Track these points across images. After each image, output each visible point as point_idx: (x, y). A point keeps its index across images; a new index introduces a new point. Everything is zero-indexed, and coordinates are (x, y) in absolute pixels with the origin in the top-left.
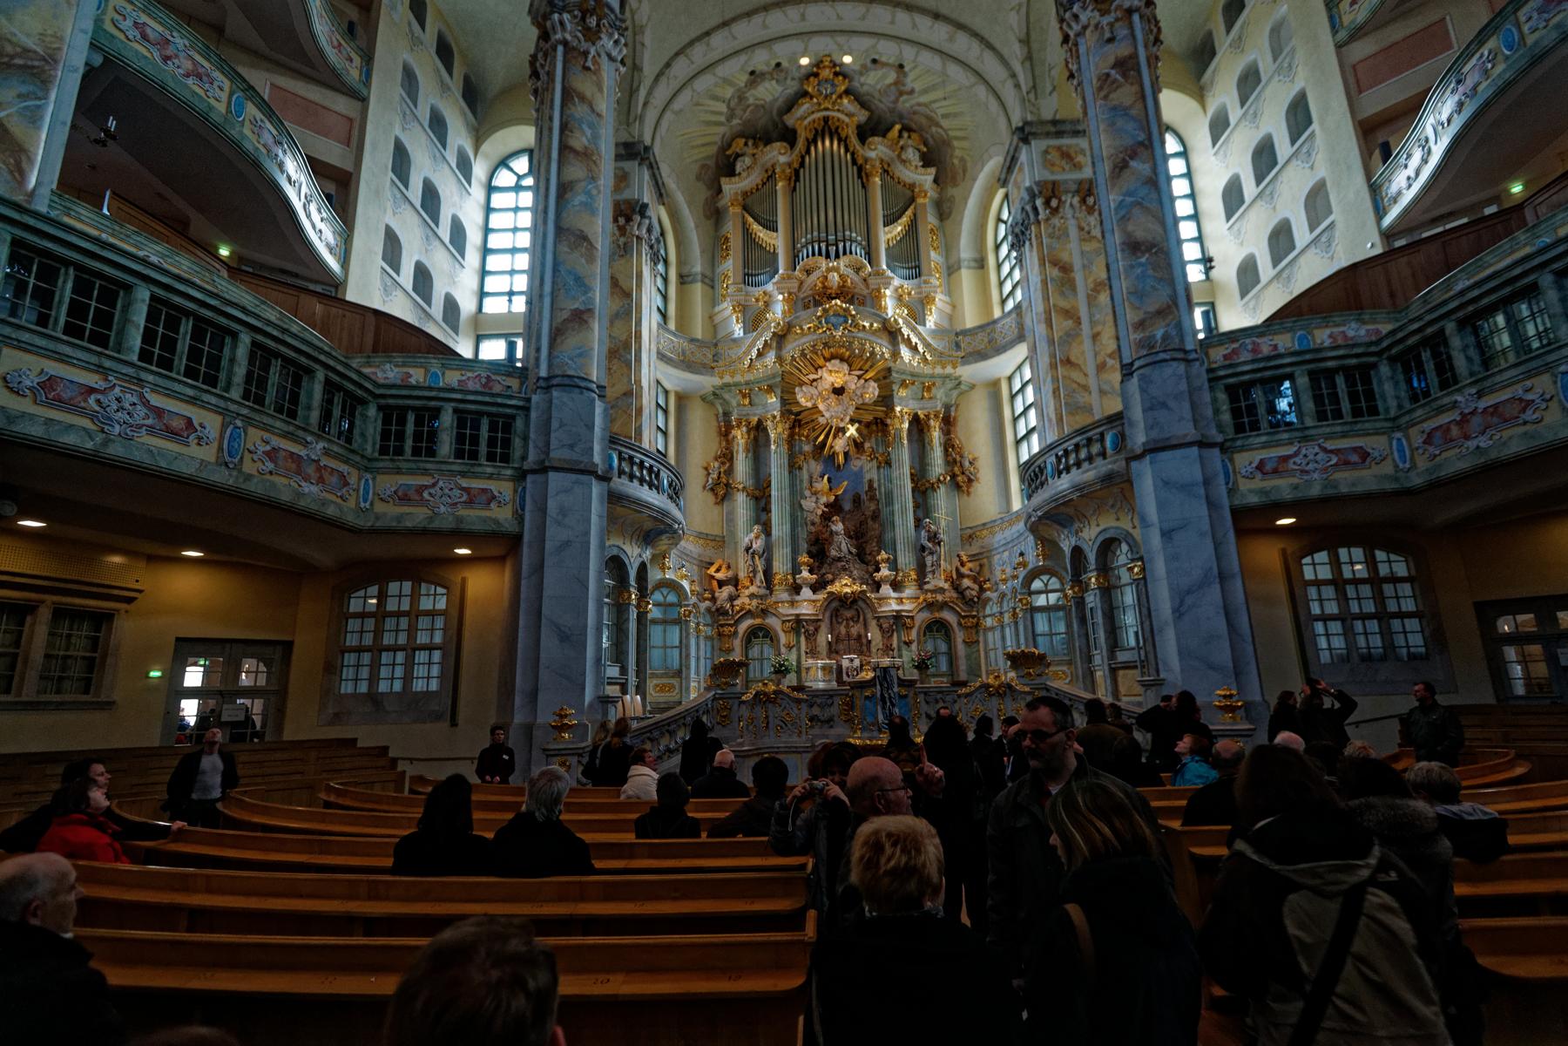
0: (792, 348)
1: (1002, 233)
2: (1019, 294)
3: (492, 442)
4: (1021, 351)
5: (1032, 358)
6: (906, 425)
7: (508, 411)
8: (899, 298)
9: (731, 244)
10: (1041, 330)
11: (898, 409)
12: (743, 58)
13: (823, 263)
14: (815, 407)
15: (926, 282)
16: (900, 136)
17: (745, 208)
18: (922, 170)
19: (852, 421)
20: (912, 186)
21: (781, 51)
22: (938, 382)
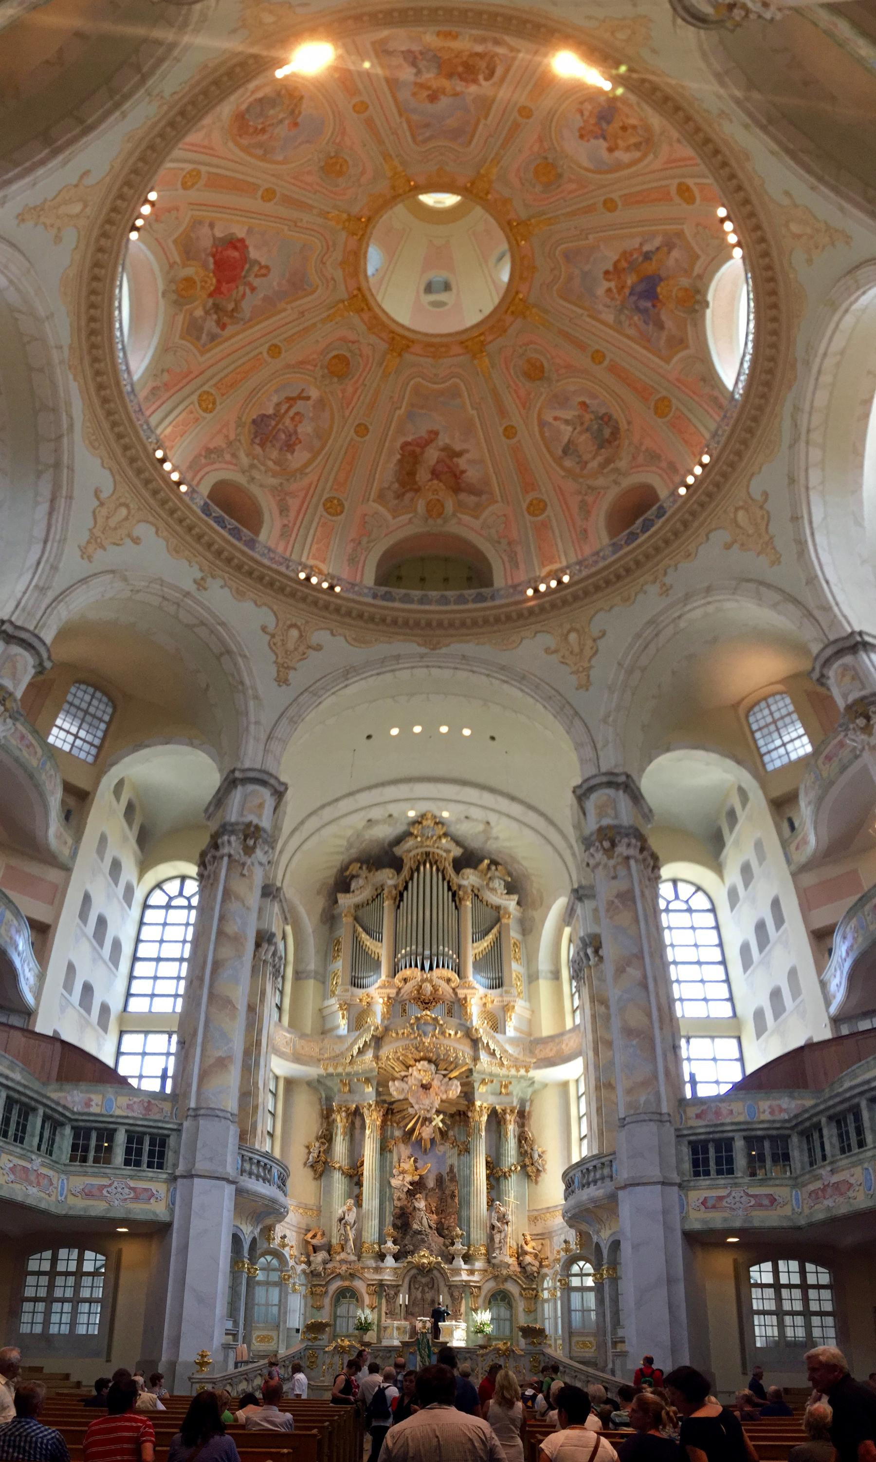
0: (387, 1051)
3: (151, 1154)
6: (485, 1118)
7: (166, 1132)
9: (343, 946)
10: (591, 1054)
11: (478, 1103)
12: (362, 814)
13: (417, 972)
14: (406, 1099)
15: (507, 992)
17: (356, 919)
18: (507, 897)
19: (438, 1112)
20: (498, 908)
21: (393, 809)
22: (514, 1082)
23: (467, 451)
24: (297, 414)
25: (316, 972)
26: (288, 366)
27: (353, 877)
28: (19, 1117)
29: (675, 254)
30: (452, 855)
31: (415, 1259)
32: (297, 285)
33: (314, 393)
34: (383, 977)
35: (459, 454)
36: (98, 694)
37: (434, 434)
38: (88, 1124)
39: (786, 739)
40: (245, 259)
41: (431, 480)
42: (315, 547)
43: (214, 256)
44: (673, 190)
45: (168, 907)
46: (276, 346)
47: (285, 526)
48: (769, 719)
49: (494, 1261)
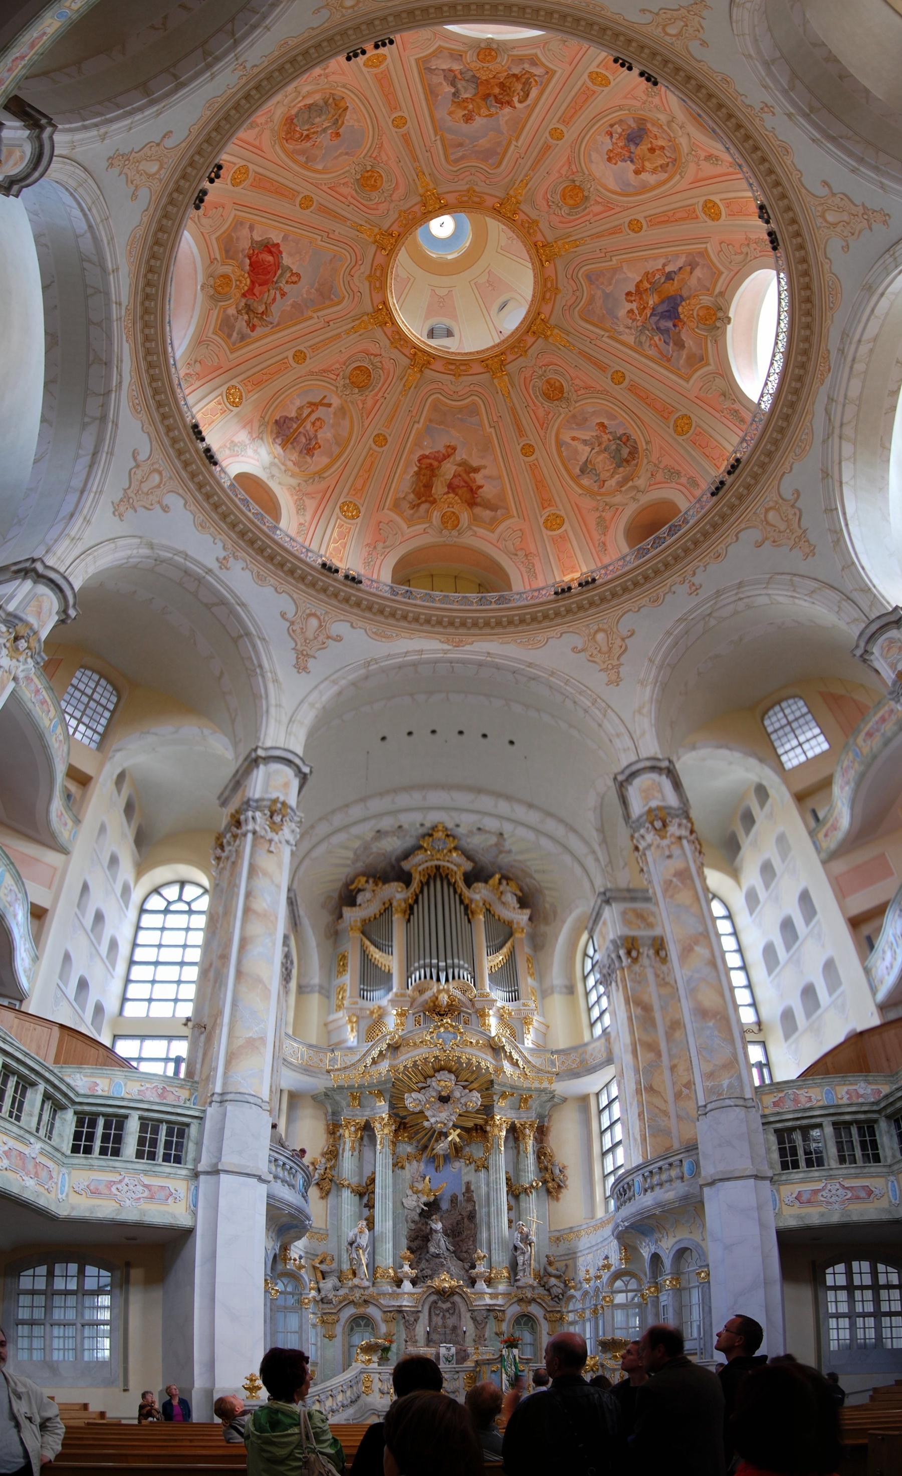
1: (588, 966)
2: (607, 1019)
4: (609, 1072)
5: (619, 1077)
8: (501, 1018)
10: (628, 1058)
12: (373, 822)
15: (524, 1005)
16: (500, 883)
17: (363, 933)
23: (485, 467)
24: (318, 419)
25: (321, 987)
26: (312, 373)
27: (359, 890)
28: (16, 1091)
29: (698, 272)
30: (462, 869)
31: (436, 1283)
32: (325, 295)
33: (336, 401)
34: (395, 990)
35: (476, 470)
36: (103, 682)
37: (451, 450)
38: (94, 1109)
39: (802, 739)
40: (278, 265)
41: (448, 493)
42: (332, 546)
43: (250, 258)
44: (699, 209)
45: (166, 911)
46: (301, 352)
47: (301, 524)
48: (784, 722)
49: (519, 1284)
